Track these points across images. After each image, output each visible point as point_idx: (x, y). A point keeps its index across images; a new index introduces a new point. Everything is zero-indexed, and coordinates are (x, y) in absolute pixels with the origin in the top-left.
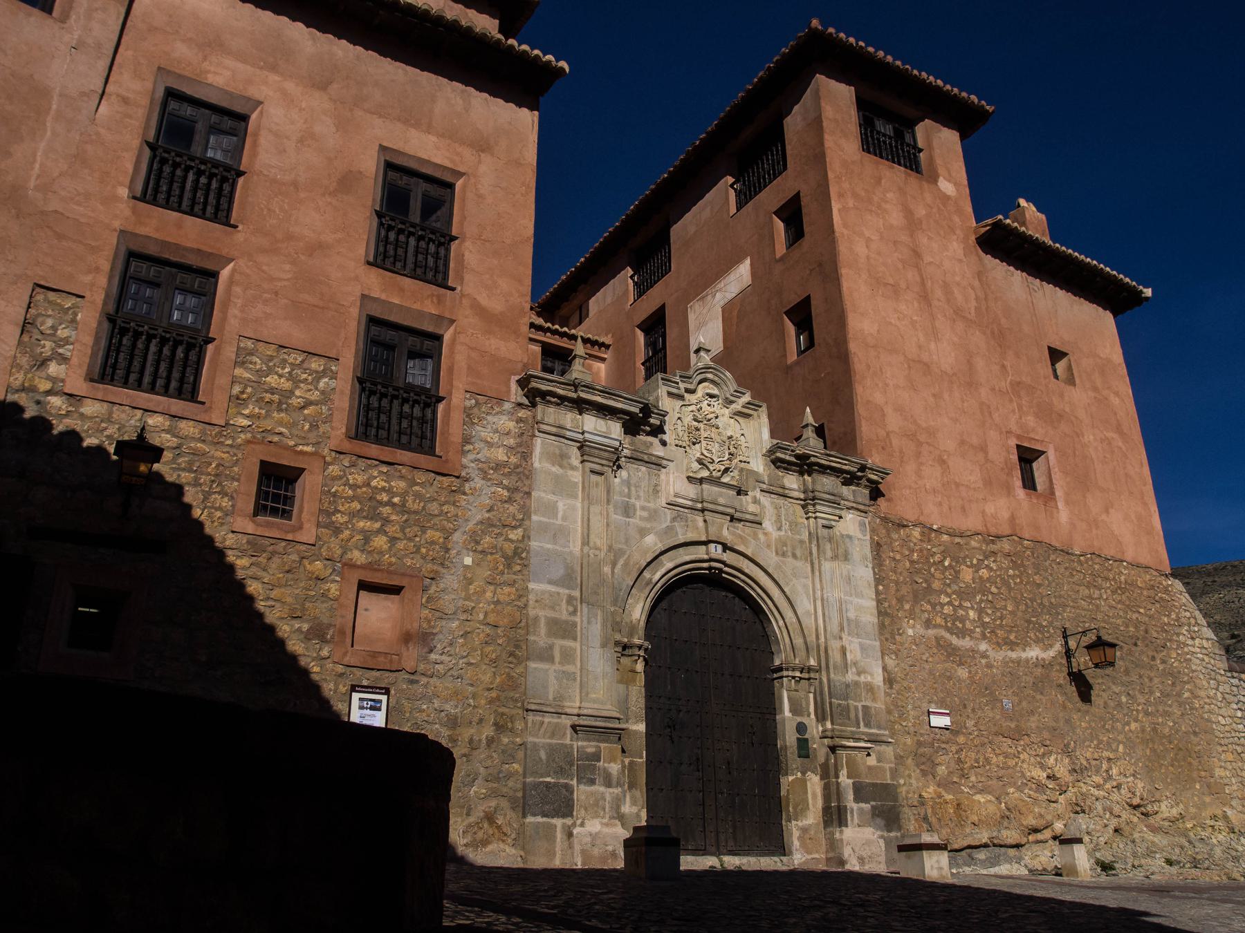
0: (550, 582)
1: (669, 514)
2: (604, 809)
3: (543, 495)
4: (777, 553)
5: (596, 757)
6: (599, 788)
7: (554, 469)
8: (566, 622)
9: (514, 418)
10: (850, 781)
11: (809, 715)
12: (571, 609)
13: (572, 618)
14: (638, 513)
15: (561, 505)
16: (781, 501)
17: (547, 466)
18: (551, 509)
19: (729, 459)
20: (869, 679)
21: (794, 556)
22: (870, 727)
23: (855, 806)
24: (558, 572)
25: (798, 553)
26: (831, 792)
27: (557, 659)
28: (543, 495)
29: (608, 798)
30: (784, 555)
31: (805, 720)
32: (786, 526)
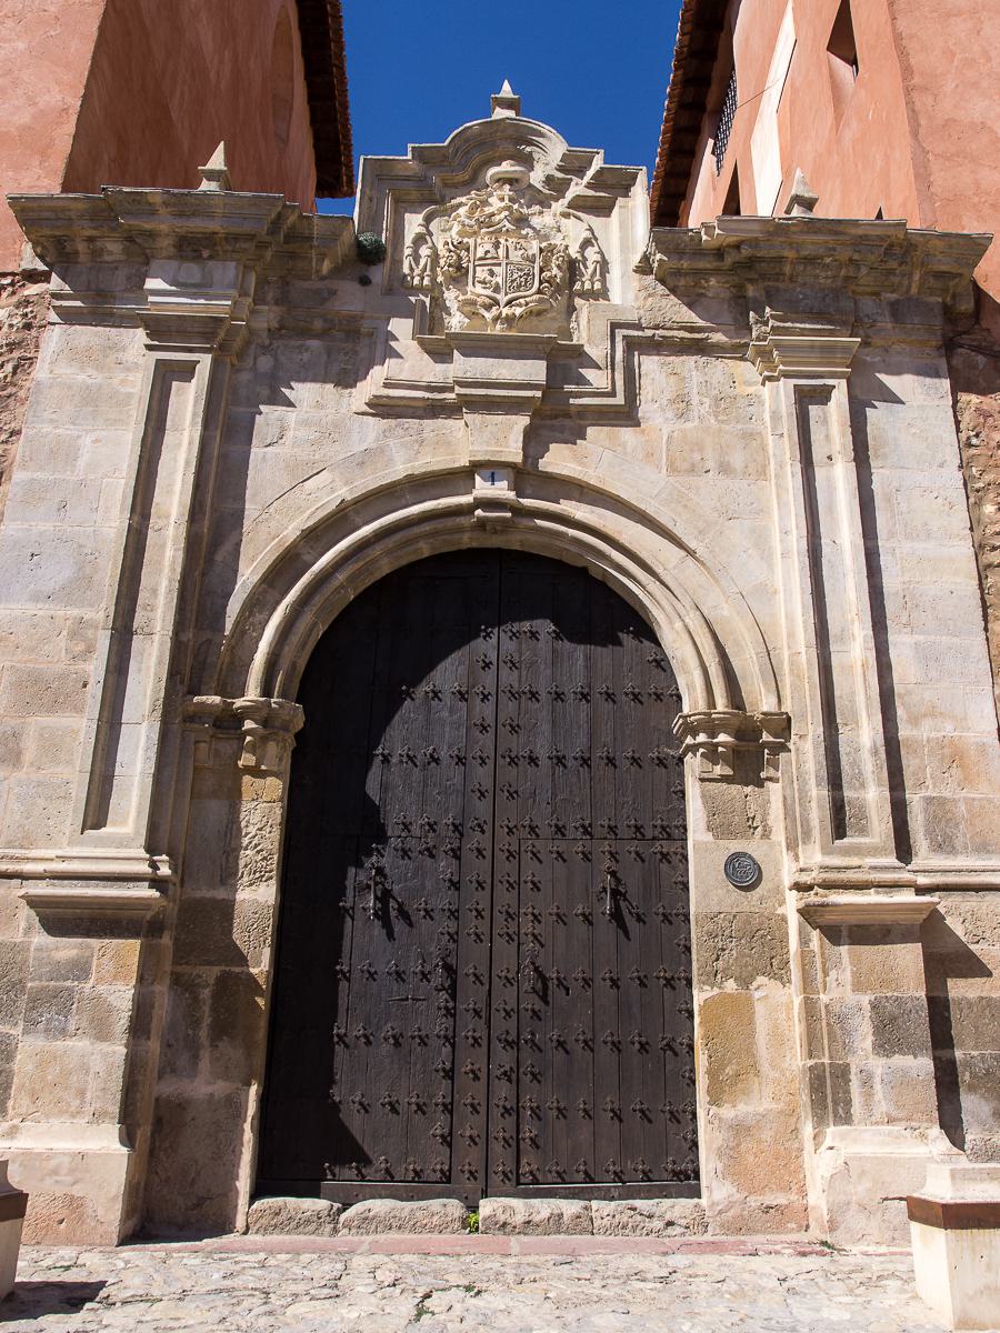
0: (35, 598)
1: (375, 425)
2: (82, 1093)
3: (47, 428)
4: (672, 468)
5: (80, 969)
6: (80, 1045)
7: (82, 377)
8: (63, 677)
9: (15, 299)
10: (865, 1000)
11: (766, 835)
12: (81, 647)
13: (81, 666)
14: (290, 434)
15: (87, 440)
16: (689, 362)
17: (66, 371)
18: (64, 453)
19: (539, 292)
20: (948, 729)
21: (725, 469)
22: (953, 851)
23: (878, 1065)
24: (57, 573)
25: (737, 459)
26: (820, 1026)
27: (28, 757)
28: (47, 428)
29: (97, 1064)
30: (692, 470)
31: (753, 847)
32: (701, 406)
